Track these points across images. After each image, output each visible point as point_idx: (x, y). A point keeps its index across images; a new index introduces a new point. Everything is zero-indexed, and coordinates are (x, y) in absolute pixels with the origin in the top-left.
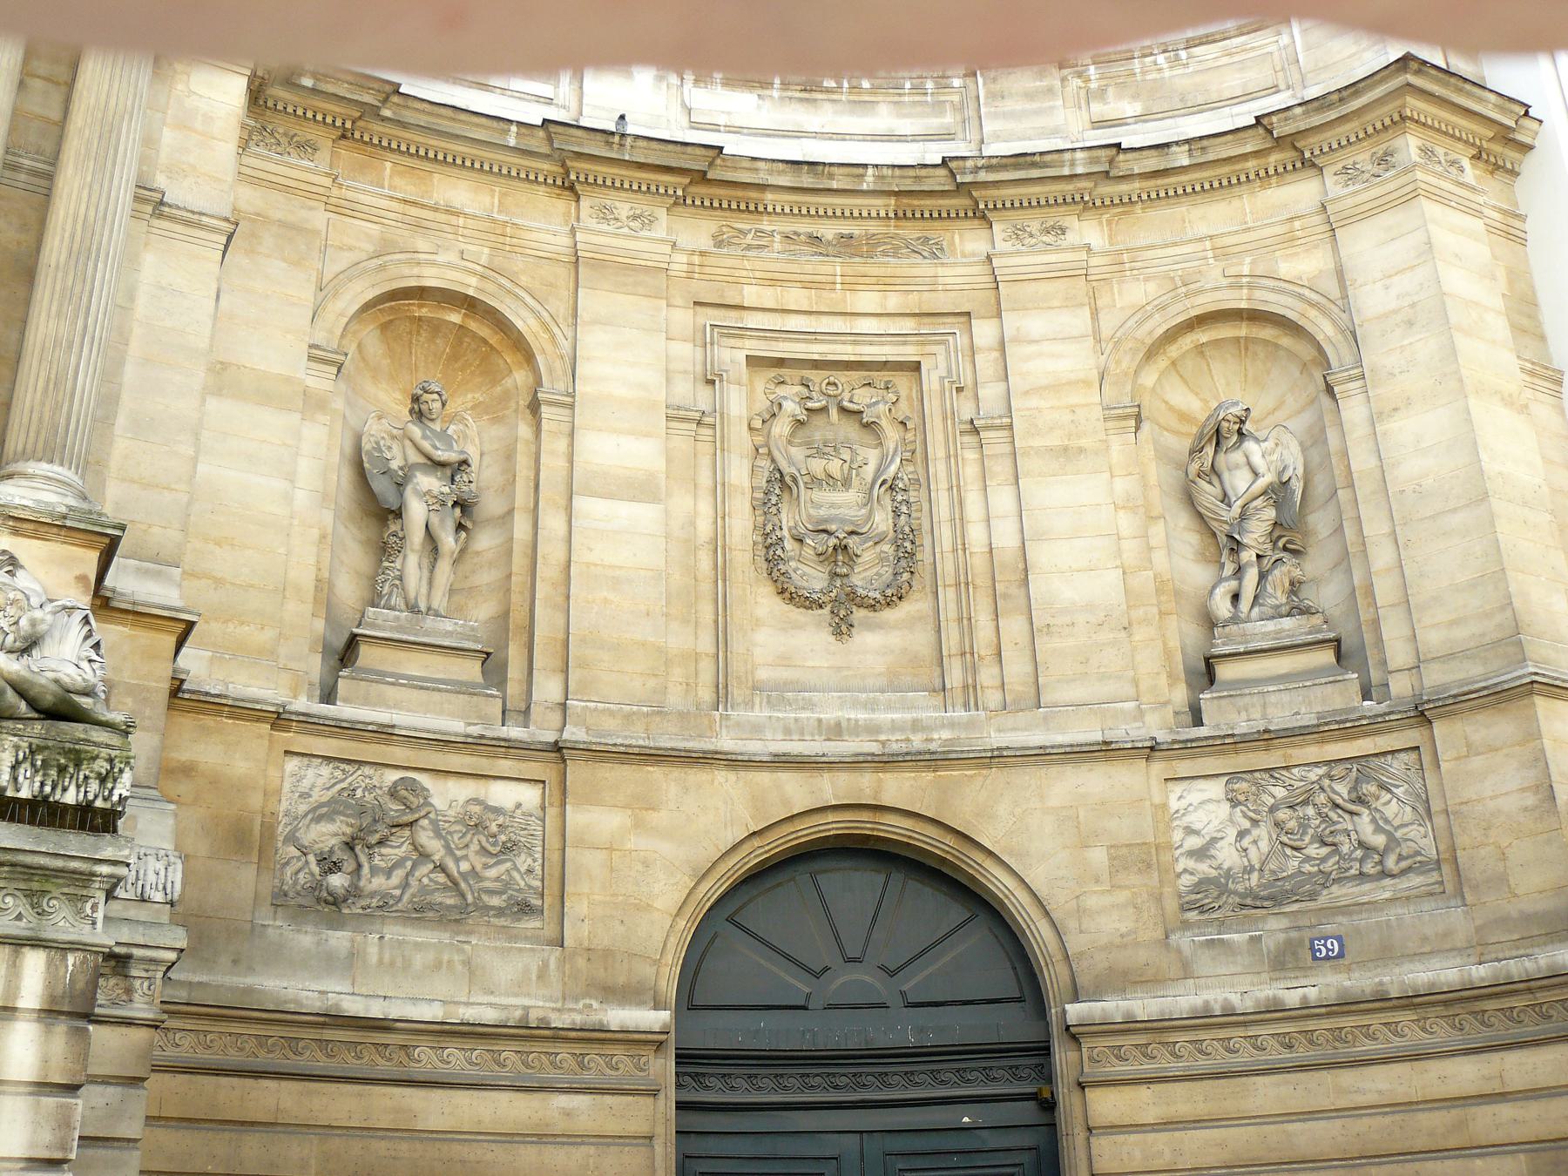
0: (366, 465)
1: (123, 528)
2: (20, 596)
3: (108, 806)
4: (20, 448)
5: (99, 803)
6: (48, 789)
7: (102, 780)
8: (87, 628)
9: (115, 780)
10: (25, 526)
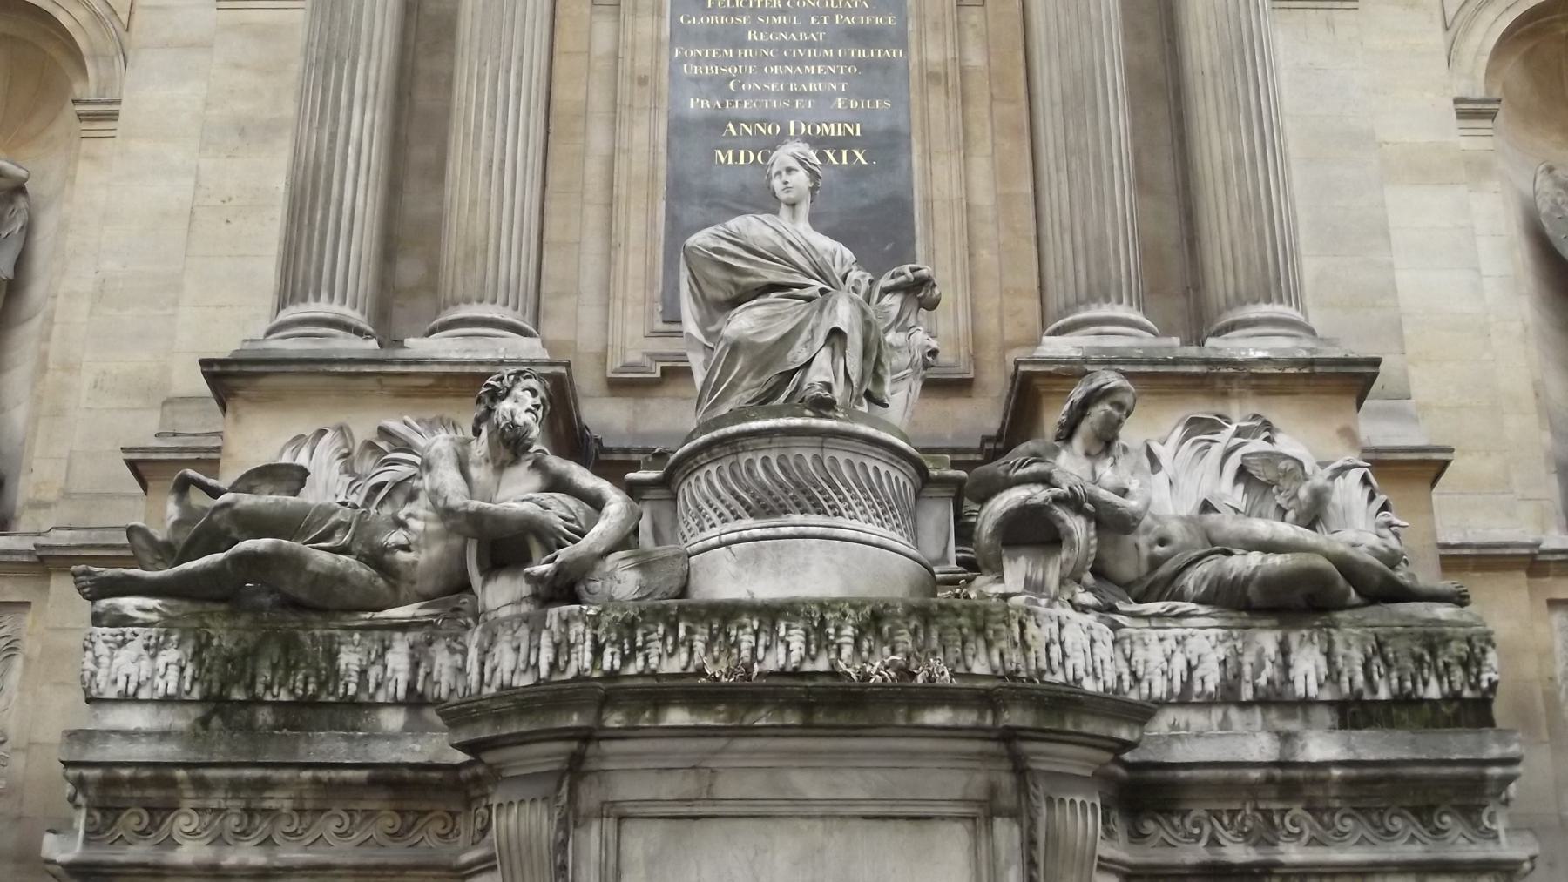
0: (1550, 232)
1: (1376, 362)
2: (1291, 465)
3: (1478, 695)
4: (1231, 292)
5: (1467, 693)
6: (1409, 684)
7: (1465, 665)
8: (1368, 490)
9: (1479, 664)
10: (1269, 382)
